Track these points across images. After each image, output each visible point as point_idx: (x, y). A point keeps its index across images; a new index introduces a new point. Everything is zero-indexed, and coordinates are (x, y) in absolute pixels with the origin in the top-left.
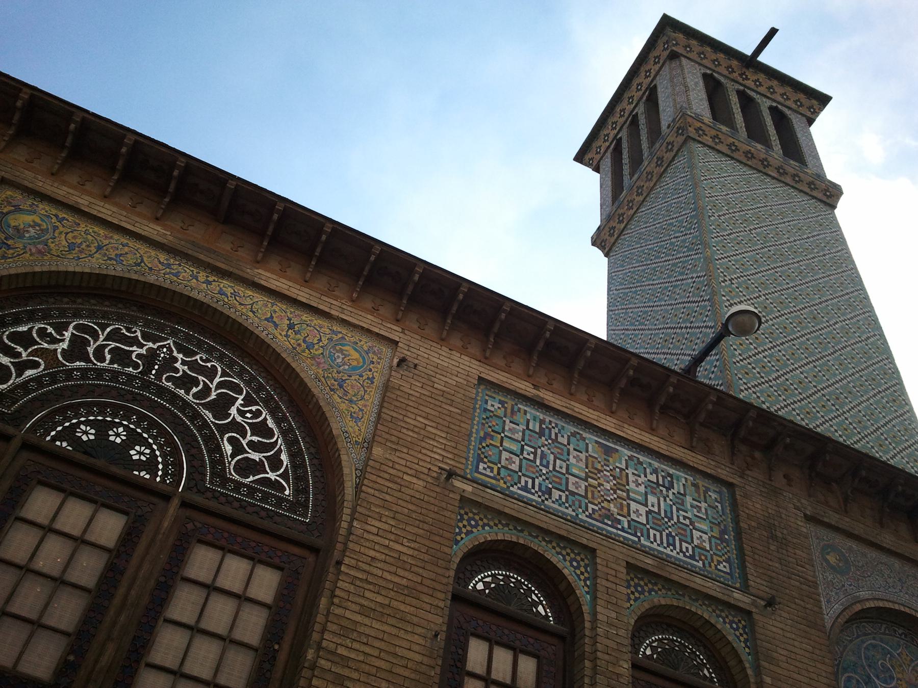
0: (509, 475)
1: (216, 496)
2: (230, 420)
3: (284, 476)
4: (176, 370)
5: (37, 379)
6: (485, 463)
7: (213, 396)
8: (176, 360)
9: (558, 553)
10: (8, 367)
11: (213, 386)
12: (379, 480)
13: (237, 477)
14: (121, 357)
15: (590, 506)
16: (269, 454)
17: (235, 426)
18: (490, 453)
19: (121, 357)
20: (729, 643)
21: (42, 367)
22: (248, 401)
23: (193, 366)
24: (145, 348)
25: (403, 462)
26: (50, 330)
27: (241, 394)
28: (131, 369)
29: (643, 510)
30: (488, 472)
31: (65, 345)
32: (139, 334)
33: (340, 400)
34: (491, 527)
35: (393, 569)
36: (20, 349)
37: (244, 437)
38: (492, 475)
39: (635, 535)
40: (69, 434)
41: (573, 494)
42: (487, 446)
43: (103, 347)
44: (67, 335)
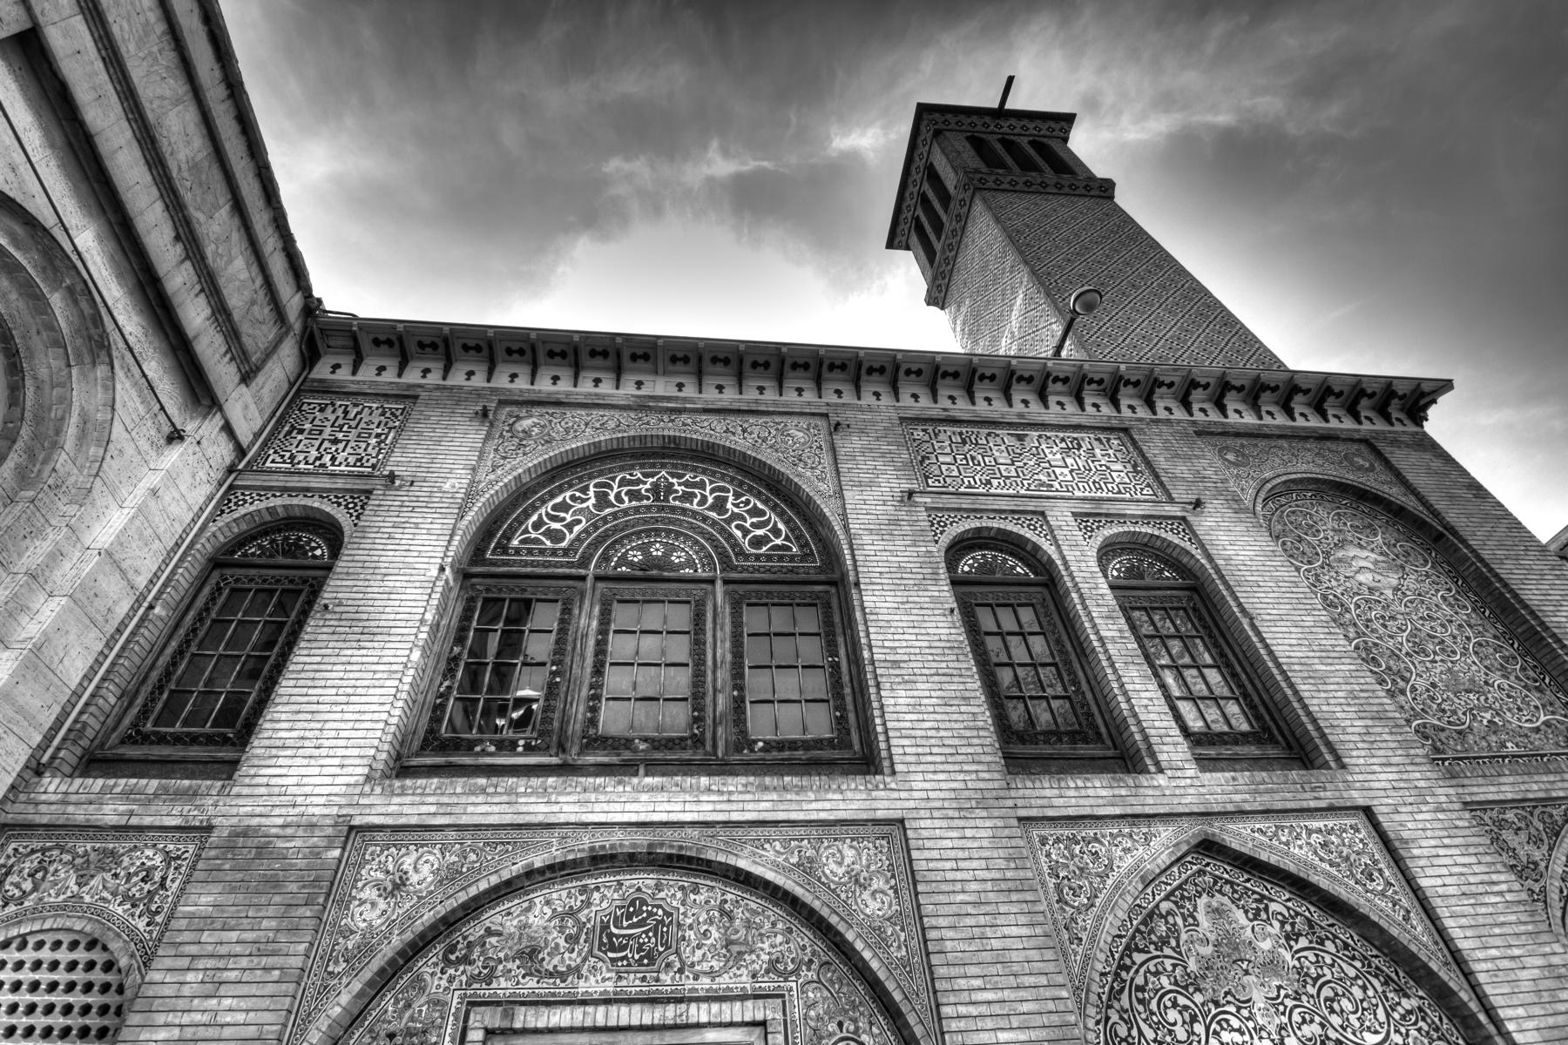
1: (745, 569)
4: (677, 491)
5: (585, 531)
8: (673, 484)
11: (707, 494)
17: (735, 516)
19: (634, 495)
20: (1177, 545)
21: (584, 521)
22: (737, 495)
23: (686, 484)
26: (578, 494)
31: (593, 501)
32: (639, 475)
36: (562, 515)
37: (746, 521)
40: (623, 560)
43: (619, 493)
44: (591, 493)
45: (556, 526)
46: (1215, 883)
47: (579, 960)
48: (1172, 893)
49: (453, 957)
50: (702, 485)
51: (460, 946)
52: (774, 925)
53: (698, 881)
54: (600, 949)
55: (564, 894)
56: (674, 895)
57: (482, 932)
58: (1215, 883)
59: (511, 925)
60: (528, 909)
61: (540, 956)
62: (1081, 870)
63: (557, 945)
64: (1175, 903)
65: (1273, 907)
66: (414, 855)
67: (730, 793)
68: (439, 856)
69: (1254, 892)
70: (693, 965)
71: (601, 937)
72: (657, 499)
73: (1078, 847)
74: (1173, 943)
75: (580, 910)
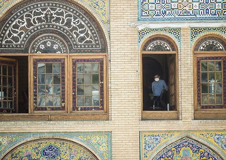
0: (152, 12)
2: (72, 27)
3: (91, 38)
4: (54, 17)
6: (144, 11)
7: (65, 21)
8: (52, 14)
9: (169, 32)
10: (17, 37)
11: (64, 18)
12: (115, 33)
13: (80, 43)
14: (39, 20)
15: (179, 11)
16: (85, 33)
17: (75, 28)
18: (145, 7)
19: (39, 20)
22: (75, 18)
23: (57, 14)
24: (44, 14)
25: (120, 24)
26: (20, 20)
27: (72, 17)
28: (43, 23)
29: (197, 4)
30: (146, 15)
31: (26, 23)
32: (40, 10)
33: (98, 10)
34: (149, 33)
35: (123, 58)
36: (17, 30)
38: (147, 15)
39: (195, 15)
41: (173, 9)
42: (144, 5)
44: (25, 20)
45: (15, 35)
46: (189, 144)
47: (39, 157)
48: (176, 146)
49: (13, 156)
50: (62, 14)
51: (14, 154)
52: (81, 151)
53: (64, 142)
54: (43, 155)
55: (34, 144)
56: (59, 145)
57: (18, 152)
58: (189, 144)
59: (24, 150)
60: (27, 147)
61: (31, 156)
62: (152, 142)
63: (34, 154)
64: (176, 148)
65: (201, 150)
66: (2, 138)
67: (71, 125)
68: (7, 138)
69: (197, 147)
70: (63, 158)
71: (43, 153)
72: (47, 21)
73: (153, 137)
74: (172, 157)
75: (38, 148)
